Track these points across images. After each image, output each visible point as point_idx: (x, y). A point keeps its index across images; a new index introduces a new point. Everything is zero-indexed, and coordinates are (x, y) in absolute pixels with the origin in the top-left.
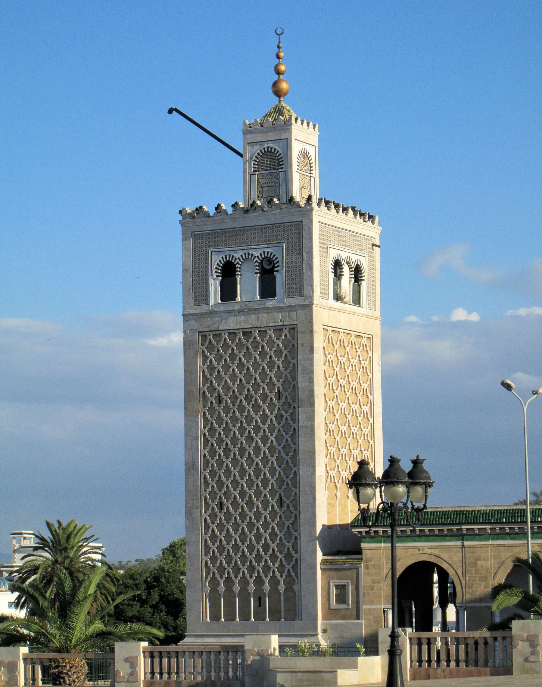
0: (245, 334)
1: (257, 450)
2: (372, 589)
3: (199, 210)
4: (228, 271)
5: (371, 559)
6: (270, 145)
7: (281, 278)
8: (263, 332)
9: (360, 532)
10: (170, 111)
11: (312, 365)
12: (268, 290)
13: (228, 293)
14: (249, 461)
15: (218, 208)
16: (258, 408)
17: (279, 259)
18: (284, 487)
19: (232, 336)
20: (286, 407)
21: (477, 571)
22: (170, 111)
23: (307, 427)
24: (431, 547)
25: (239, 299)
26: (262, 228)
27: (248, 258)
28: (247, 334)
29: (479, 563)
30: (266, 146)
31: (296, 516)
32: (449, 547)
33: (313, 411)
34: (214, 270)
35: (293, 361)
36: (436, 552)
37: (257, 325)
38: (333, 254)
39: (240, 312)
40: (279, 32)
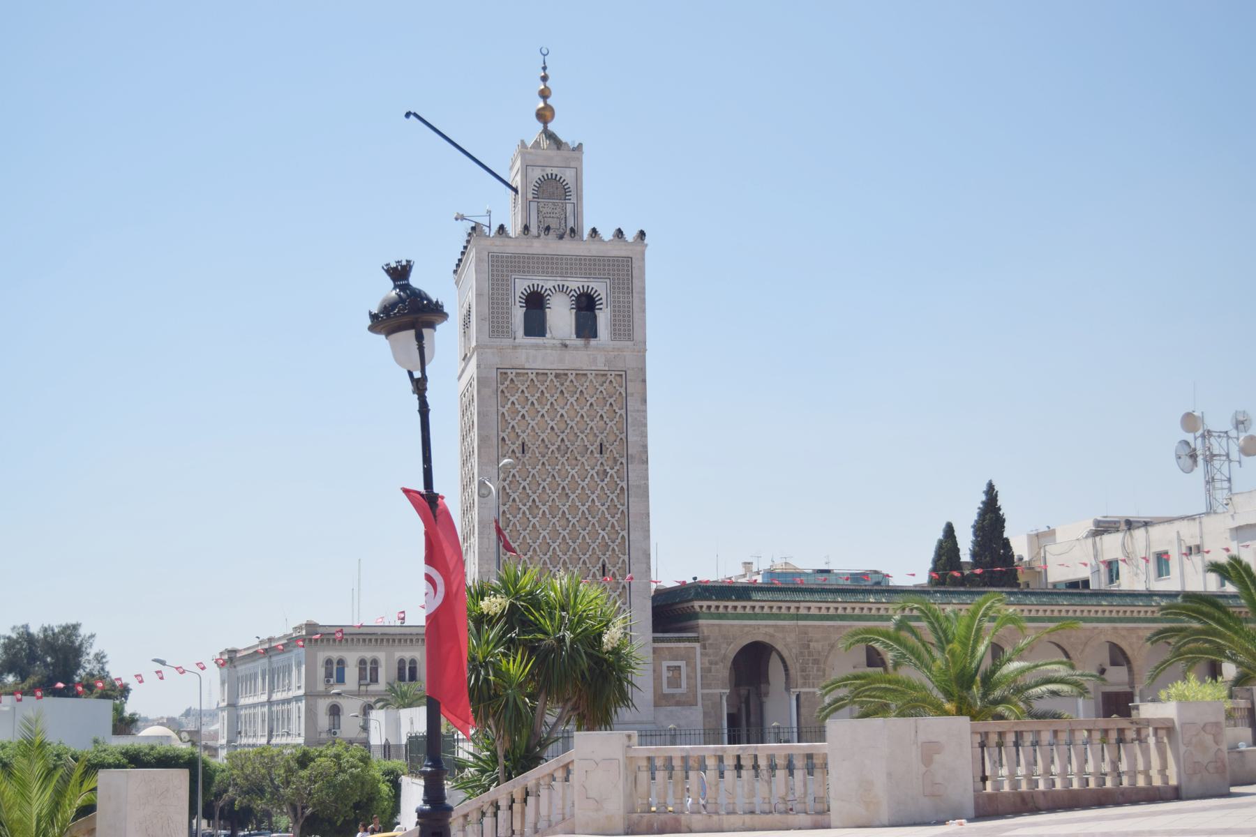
0: (557, 376)
1: (574, 507)
2: (710, 670)
4: (536, 302)
5: (708, 638)
6: (555, 171)
7: (603, 318)
8: (581, 375)
9: (701, 607)
10: (408, 115)
11: (645, 418)
12: (586, 327)
13: (536, 324)
14: (564, 522)
16: (574, 462)
17: (603, 296)
18: (608, 553)
19: (540, 378)
20: (610, 463)
21: (810, 654)
22: (408, 115)
23: (639, 487)
24: (766, 626)
25: (548, 335)
26: (580, 259)
29: (812, 644)
30: (549, 171)
31: (624, 587)
32: (783, 627)
33: (647, 470)
34: (518, 299)
35: (619, 412)
36: (771, 630)
37: (577, 366)
39: (554, 347)
40: (545, 52)
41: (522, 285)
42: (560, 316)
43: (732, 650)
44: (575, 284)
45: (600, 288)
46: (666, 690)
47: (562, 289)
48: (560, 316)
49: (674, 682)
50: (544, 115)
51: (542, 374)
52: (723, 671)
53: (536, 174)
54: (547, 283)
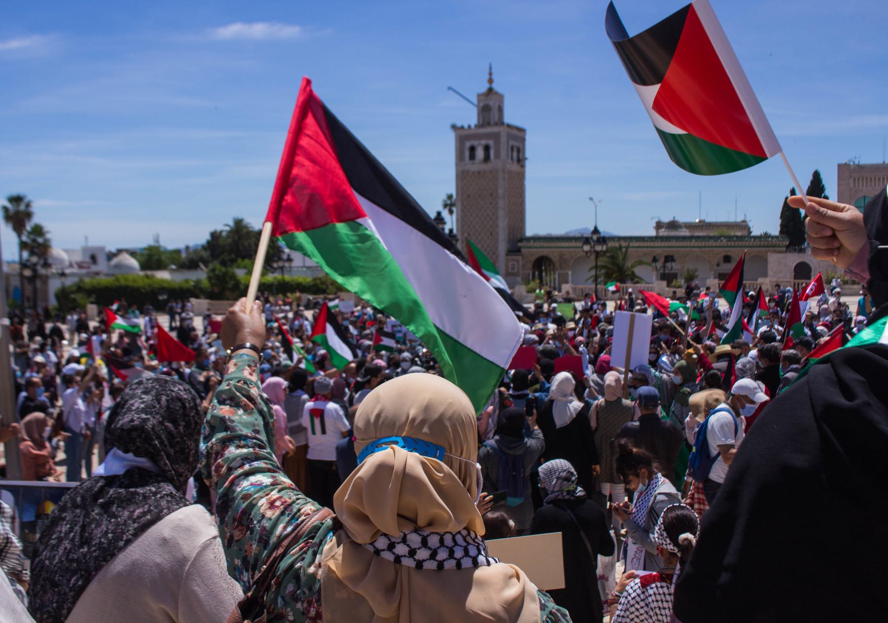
3: (462, 128)
4: (472, 149)
8: (485, 172)
10: (449, 88)
13: (472, 157)
15: (469, 127)
27: (479, 144)
28: (479, 173)
38: (511, 143)
41: (468, 144)
42: (480, 153)
43: (533, 259)
44: (484, 142)
45: (491, 143)
46: (510, 271)
47: (479, 144)
48: (480, 153)
49: (513, 269)
50: (491, 81)
51: (474, 173)
52: (530, 265)
53: (482, 104)
54: (475, 143)
